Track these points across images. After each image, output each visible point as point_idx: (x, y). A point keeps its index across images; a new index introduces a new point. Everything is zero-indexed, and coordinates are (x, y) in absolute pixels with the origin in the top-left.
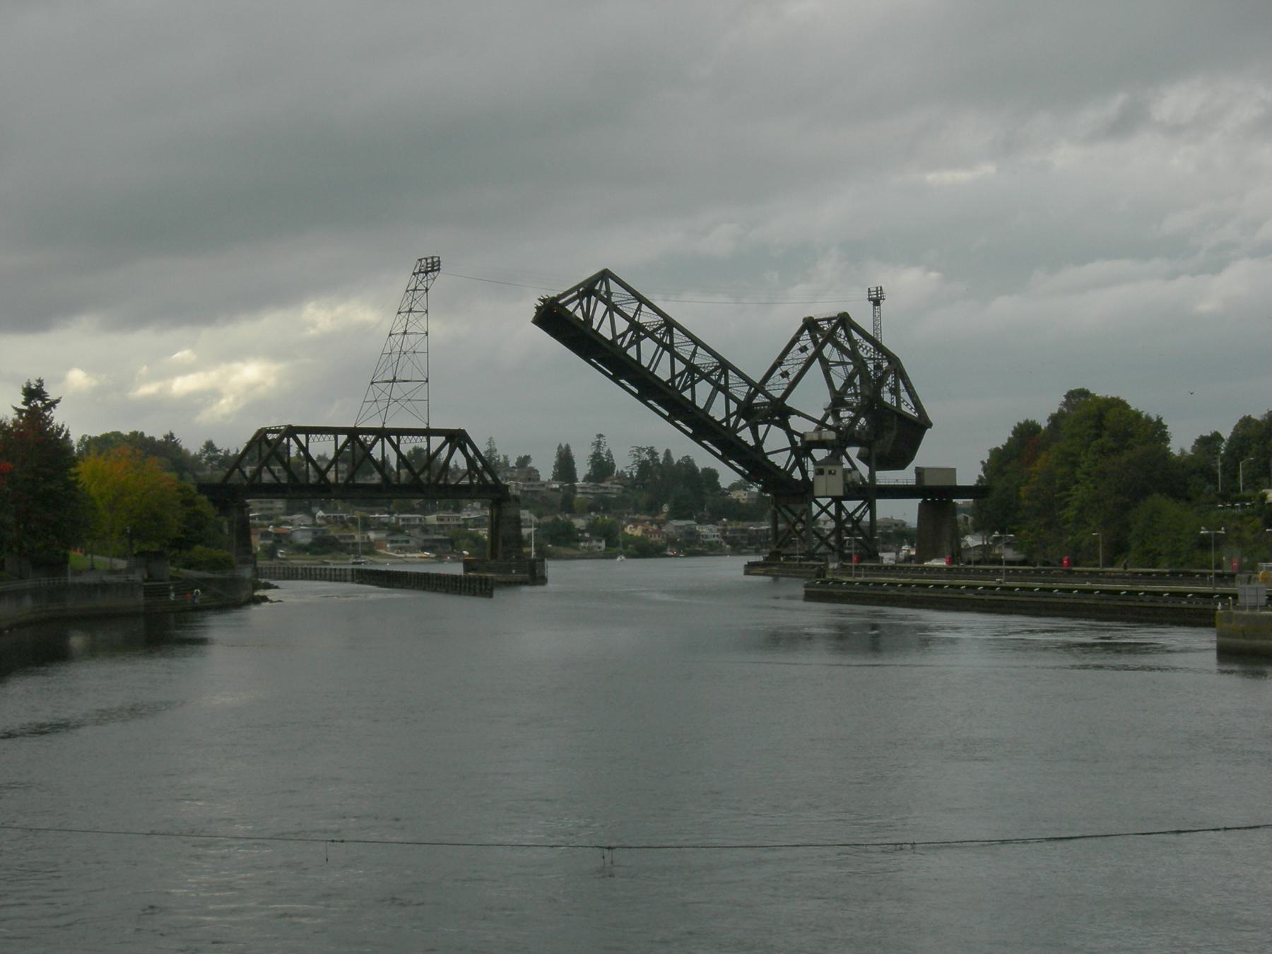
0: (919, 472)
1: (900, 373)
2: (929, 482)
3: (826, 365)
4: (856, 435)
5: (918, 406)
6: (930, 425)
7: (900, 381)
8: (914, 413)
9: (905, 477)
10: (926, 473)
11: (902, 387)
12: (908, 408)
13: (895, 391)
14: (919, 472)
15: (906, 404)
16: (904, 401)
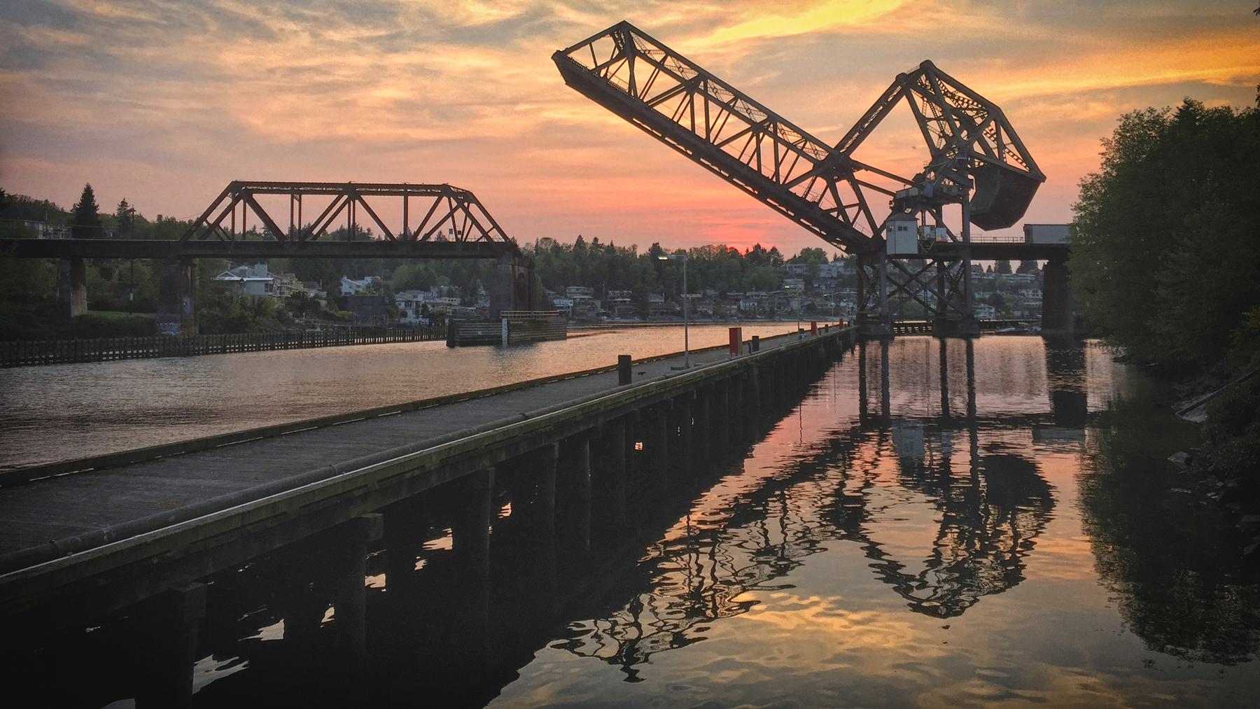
0: (1028, 229)
1: (1002, 122)
2: (1038, 240)
3: (922, 121)
4: (945, 191)
5: (1026, 158)
6: (1043, 178)
7: (1002, 128)
8: (1025, 167)
9: (1013, 234)
10: (1034, 227)
11: (1006, 139)
12: (1012, 161)
13: (1001, 146)
14: (1028, 229)
15: (1011, 154)
16: (1010, 151)
